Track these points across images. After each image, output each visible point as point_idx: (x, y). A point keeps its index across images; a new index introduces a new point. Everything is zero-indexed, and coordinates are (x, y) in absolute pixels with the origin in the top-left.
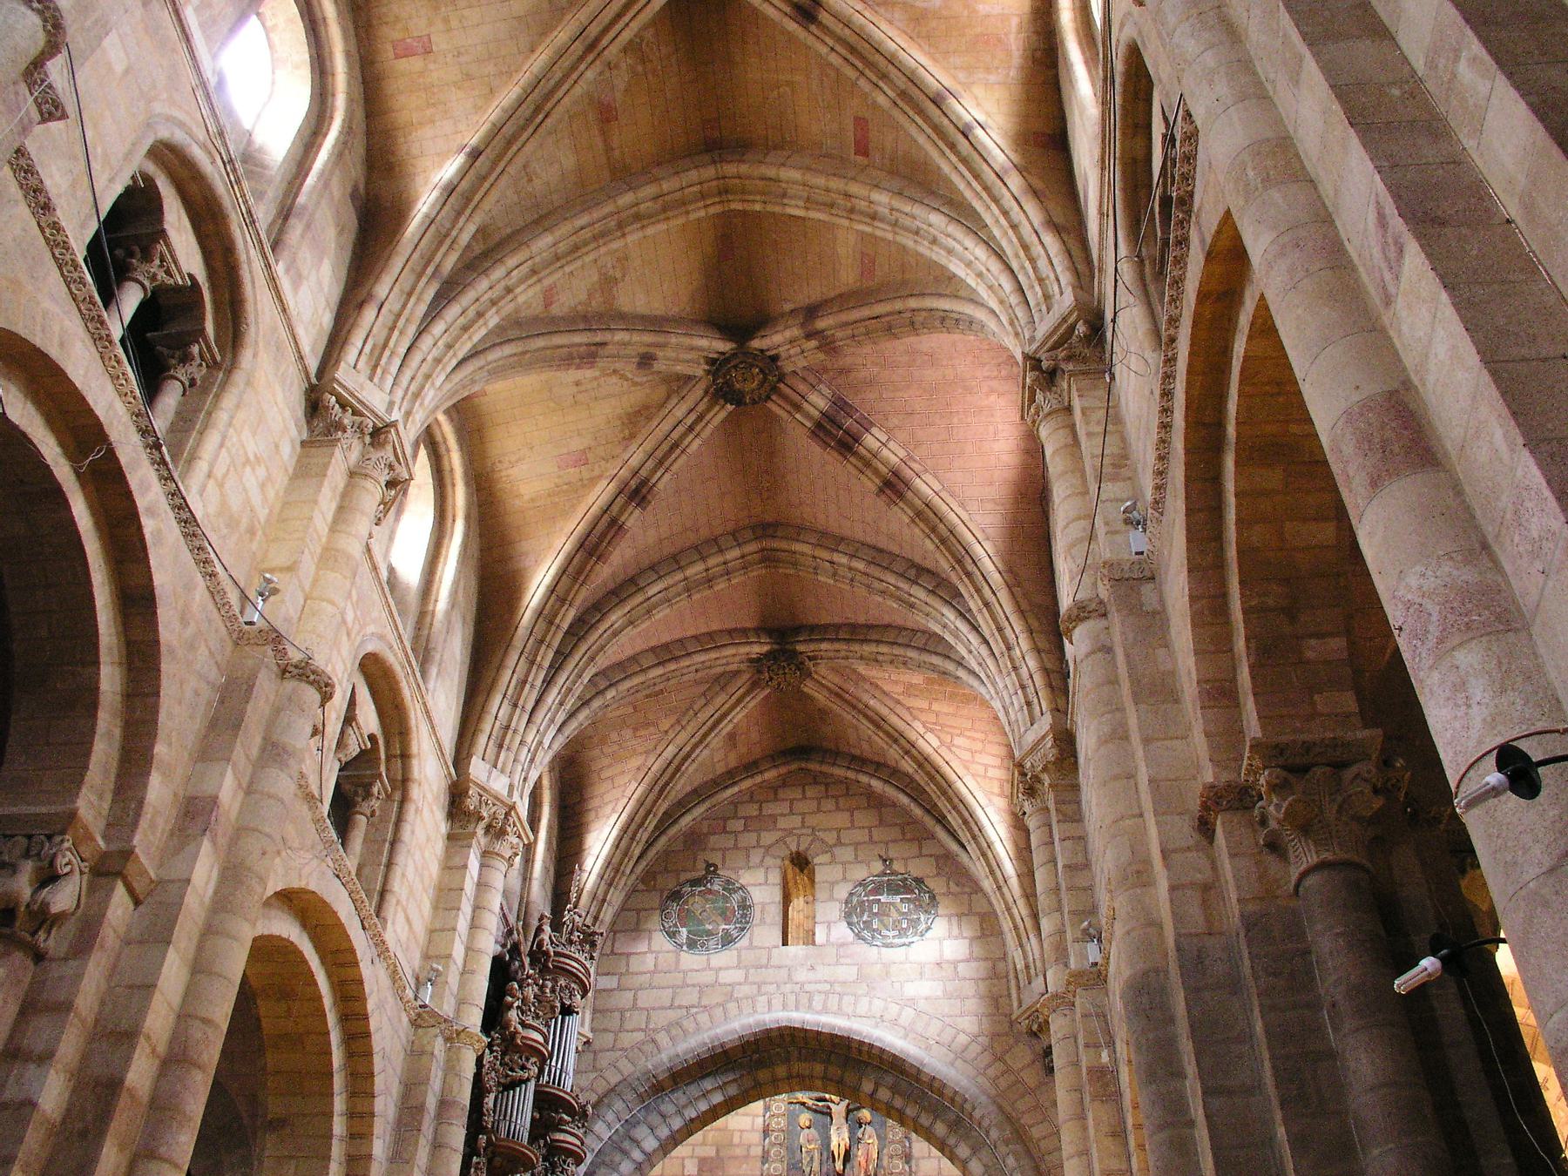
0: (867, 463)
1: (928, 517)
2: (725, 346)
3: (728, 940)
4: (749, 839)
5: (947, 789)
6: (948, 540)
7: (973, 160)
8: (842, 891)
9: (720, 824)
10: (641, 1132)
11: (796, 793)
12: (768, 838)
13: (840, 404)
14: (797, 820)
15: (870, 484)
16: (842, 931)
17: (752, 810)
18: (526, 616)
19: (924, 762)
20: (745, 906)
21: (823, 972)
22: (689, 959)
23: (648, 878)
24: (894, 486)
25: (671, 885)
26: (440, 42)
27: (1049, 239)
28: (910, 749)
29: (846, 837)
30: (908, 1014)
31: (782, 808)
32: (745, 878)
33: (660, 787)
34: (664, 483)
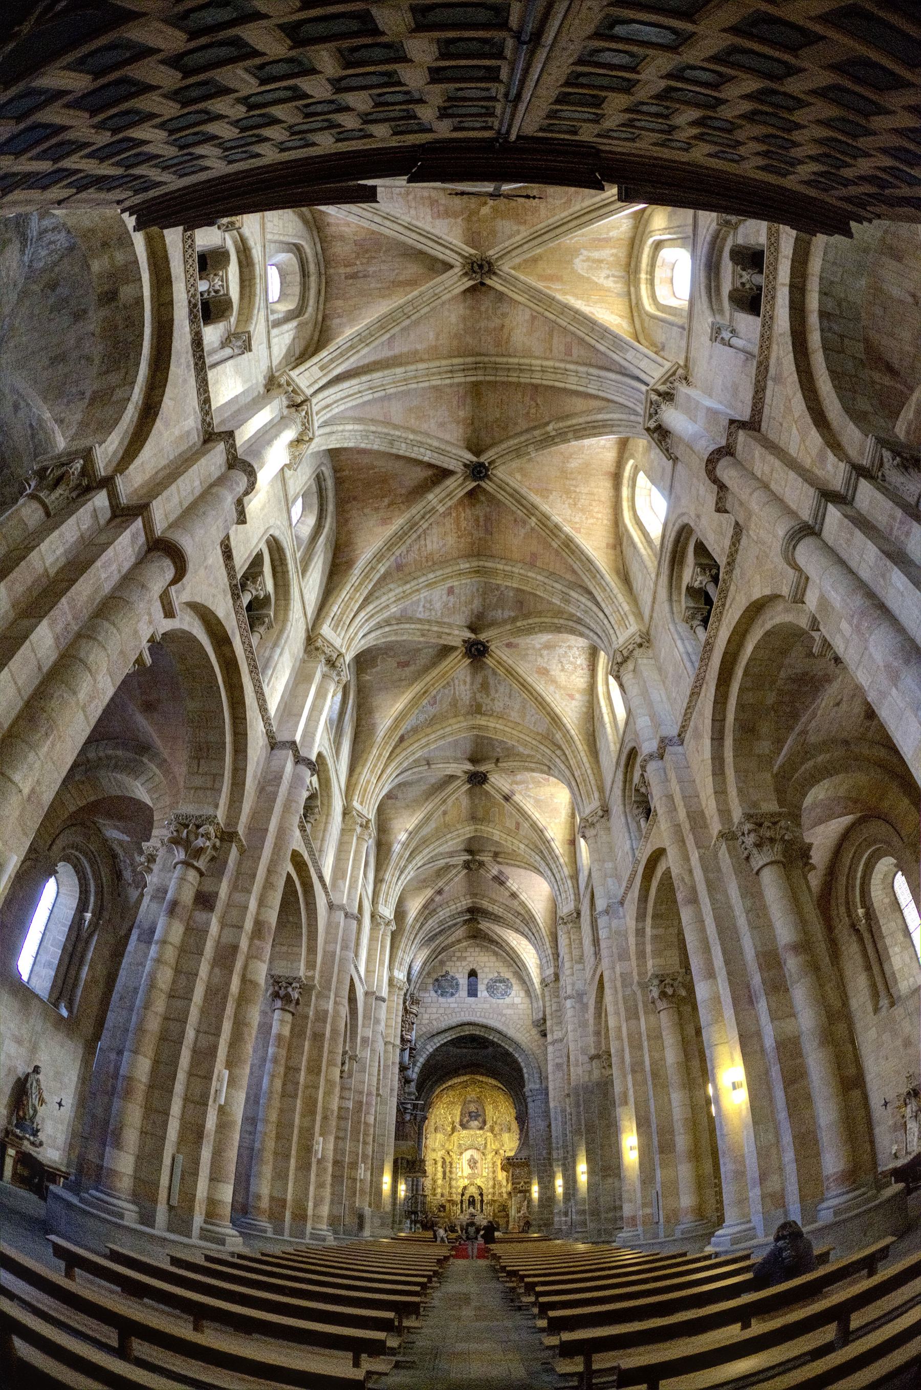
0: (507, 889)
1: (523, 904)
2: (470, 857)
3: (452, 995)
4: (458, 964)
5: (518, 956)
6: (529, 911)
7: (551, 850)
8: (486, 982)
9: (450, 959)
10: (428, 1047)
11: (472, 950)
12: (464, 963)
13: (501, 872)
14: (471, 959)
15: (507, 894)
16: (485, 993)
17: (458, 954)
18: (408, 928)
19: (512, 948)
20: (457, 984)
21: (480, 1006)
22: (441, 1000)
23: (429, 974)
24: (514, 895)
25: (435, 976)
26: (400, 796)
27: (569, 882)
28: (508, 944)
29: (488, 964)
30: (503, 1019)
31: (468, 954)
32: (457, 976)
33: (434, 951)
34: (447, 888)
